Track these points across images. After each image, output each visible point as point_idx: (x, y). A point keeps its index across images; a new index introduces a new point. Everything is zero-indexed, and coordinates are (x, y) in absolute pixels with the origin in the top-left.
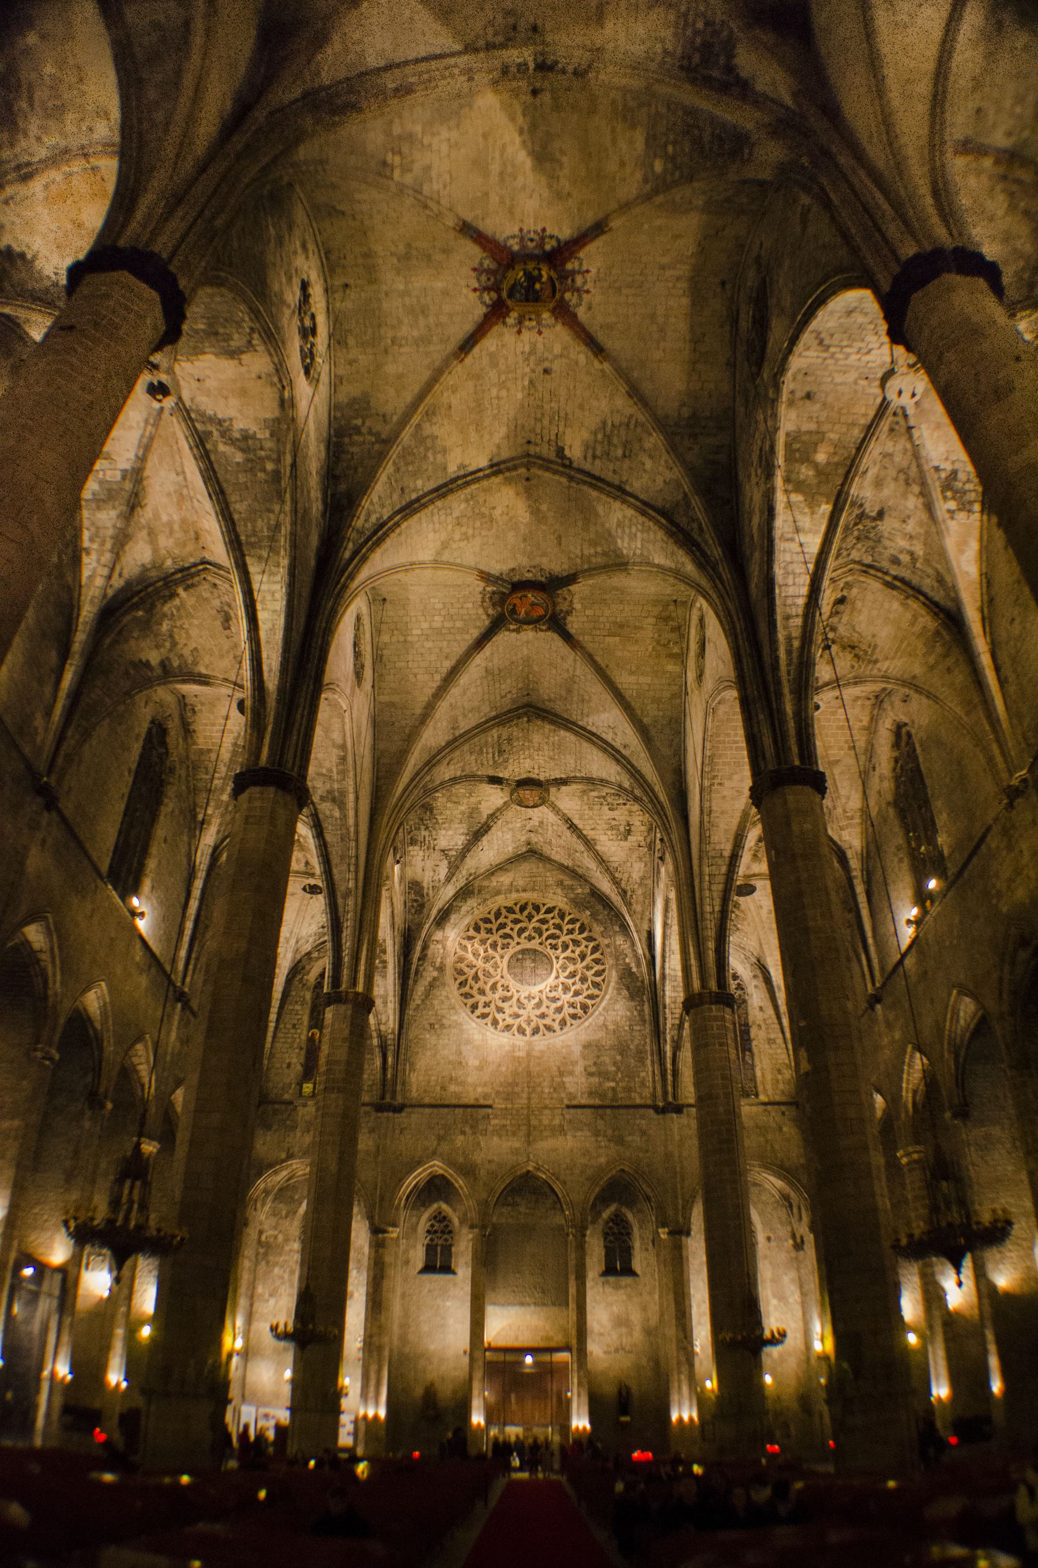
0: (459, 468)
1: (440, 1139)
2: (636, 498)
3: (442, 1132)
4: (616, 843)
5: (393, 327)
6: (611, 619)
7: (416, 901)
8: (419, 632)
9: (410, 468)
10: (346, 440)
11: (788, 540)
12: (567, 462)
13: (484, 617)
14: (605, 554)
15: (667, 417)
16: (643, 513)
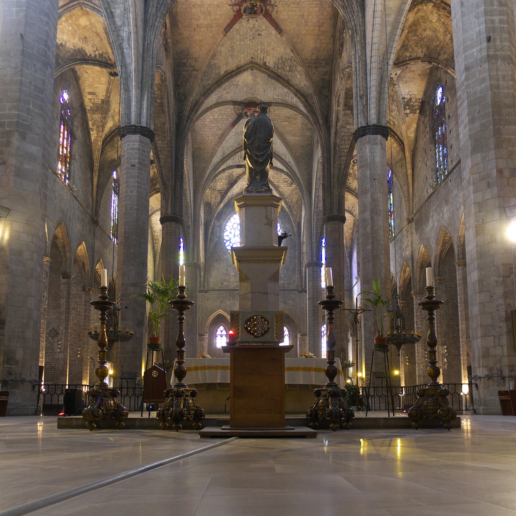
0: (225, 72)
1: (221, 302)
2: (294, 88)
3: (222, 300)
4: (287, 187)
5: (197, 20)
6: (286, 115)
7: (209, 210)
8: (209, 120)
9: (206, 78)
10: (181, 69)
11: (343, 128)
12: (268, 68)
13: (235, 114)
14: (282, 99)
15: (306, 59)
16: (296, 95)
